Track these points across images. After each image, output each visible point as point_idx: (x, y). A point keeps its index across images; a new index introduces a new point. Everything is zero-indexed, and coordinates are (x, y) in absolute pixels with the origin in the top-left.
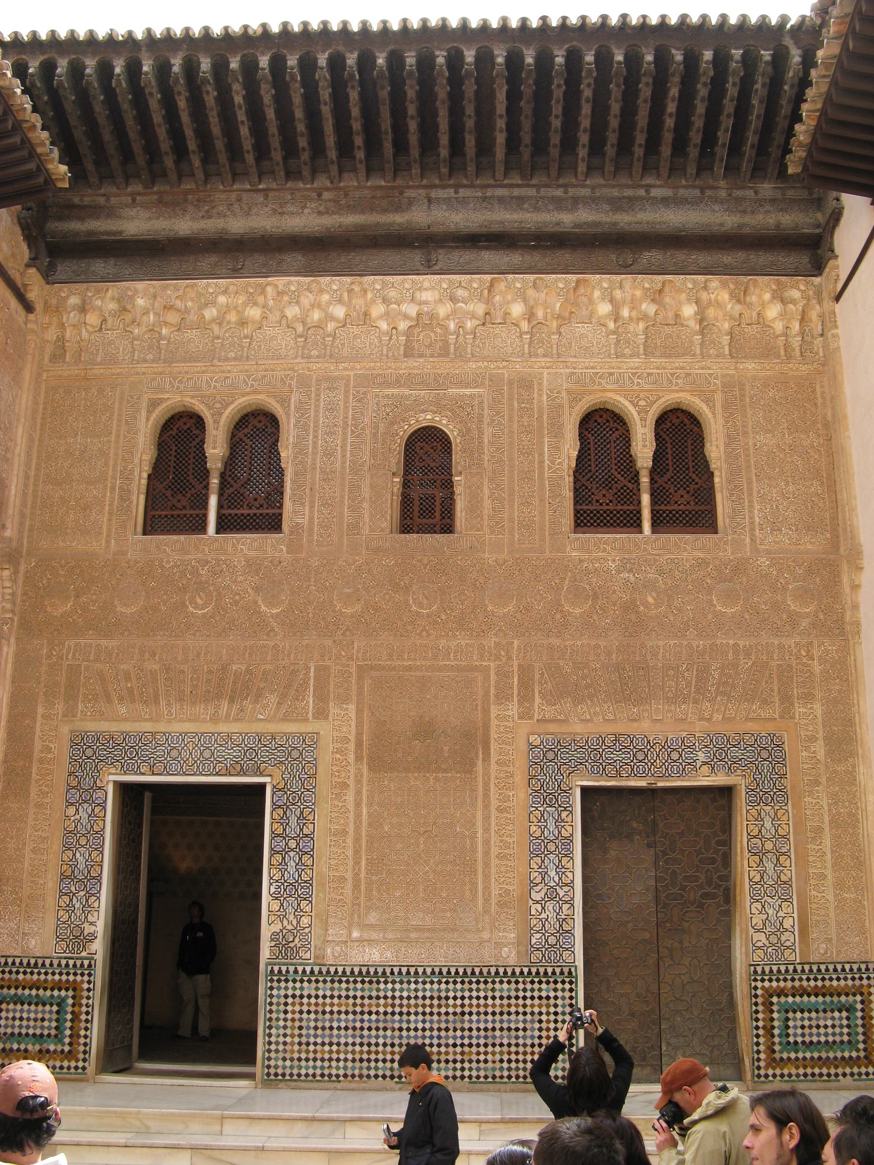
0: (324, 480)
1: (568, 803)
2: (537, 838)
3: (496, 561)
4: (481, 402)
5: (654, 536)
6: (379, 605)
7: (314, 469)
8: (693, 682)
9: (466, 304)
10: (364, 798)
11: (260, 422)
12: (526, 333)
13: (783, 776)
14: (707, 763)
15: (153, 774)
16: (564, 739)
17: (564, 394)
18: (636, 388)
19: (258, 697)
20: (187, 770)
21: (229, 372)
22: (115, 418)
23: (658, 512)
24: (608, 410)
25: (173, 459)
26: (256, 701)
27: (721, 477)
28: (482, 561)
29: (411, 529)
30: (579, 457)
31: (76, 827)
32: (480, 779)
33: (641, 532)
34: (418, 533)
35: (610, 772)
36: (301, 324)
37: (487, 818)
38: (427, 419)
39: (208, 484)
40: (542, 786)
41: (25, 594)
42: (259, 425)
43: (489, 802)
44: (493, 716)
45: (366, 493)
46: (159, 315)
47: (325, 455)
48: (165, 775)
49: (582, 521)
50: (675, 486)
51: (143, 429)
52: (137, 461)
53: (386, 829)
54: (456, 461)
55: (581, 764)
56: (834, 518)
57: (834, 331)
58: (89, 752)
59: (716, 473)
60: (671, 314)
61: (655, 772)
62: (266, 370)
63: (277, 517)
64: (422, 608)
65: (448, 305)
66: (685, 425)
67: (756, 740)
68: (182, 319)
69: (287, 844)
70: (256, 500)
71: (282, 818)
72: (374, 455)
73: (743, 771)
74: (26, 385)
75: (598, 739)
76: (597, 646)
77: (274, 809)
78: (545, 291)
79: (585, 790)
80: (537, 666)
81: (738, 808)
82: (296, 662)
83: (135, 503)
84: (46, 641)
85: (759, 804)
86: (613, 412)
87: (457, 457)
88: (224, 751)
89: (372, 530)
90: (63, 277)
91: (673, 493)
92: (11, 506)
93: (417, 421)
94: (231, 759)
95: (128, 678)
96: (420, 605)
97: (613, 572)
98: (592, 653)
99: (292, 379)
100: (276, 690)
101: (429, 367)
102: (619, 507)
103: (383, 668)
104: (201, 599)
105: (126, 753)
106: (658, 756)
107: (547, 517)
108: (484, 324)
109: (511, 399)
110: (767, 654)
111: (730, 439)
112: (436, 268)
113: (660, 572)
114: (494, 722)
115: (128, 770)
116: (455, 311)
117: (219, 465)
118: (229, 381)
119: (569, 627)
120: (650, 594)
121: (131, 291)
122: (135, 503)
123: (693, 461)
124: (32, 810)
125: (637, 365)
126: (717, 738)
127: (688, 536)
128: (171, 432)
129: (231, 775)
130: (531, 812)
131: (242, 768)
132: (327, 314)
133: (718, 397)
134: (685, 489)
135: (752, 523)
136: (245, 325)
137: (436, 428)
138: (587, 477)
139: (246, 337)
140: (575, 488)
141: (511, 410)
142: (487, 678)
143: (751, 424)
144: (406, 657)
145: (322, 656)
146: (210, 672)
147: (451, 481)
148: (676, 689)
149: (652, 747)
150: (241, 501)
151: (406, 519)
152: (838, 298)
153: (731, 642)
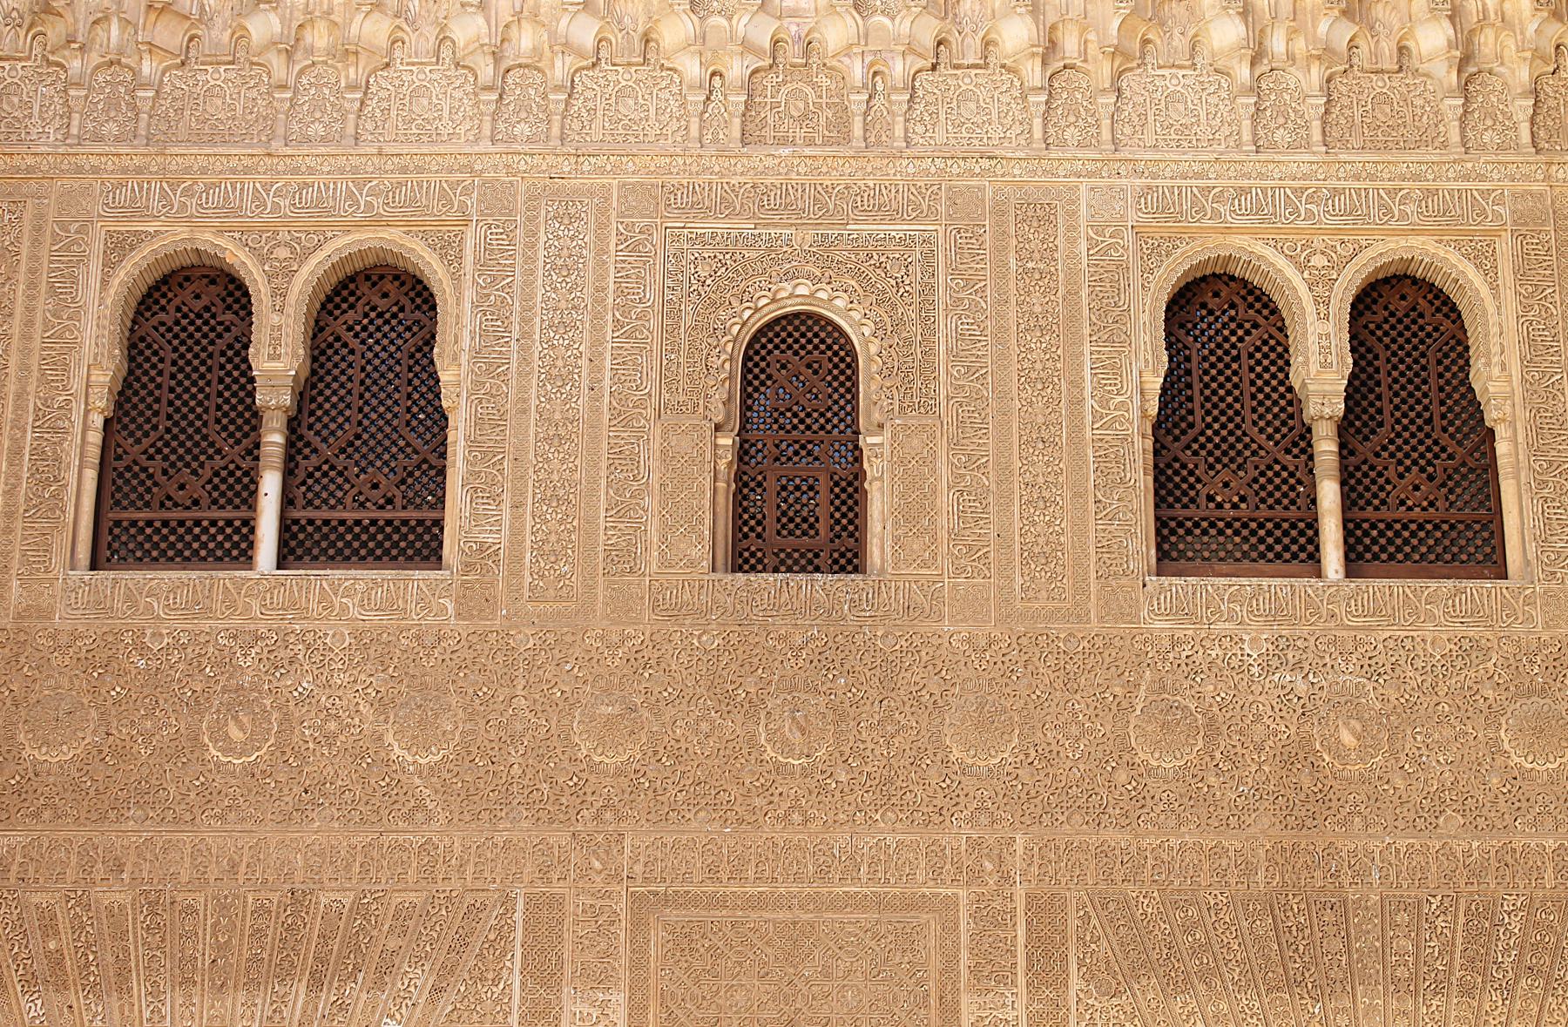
3: (969, 641)
5: (1353, 584)
7: (524, 411)
8: (1459, 941)
9: (893, 19)
11: (385, 295)
17: (1129, 236)
18: (1303, 224)
19: (385, 971)
21: (311, 171)
22: (22, 277)
23: (1358, 526)
24: (1232, 278)
26: (379, 984)
27: (1514, 440)
30: (1164, 390)
34: (776, 570)
36: (490, 60)
38: (796, 295)
39: (257, 446)
42: (382, 304)
45: (653, 470)
46: (136, 27)
50: (1400, 463)
51: (93, 308)
52: (77, 385)
54: (867, 396)
59: (1501, 432)
60: (1388, 47)
62: (404, 170)
63: (428, 530)
65: (849, 20)
66: (1421, 315)
68: (191, 39)
70: (375, 486)
72: (668, 380)
76: (1217, 852)
80: (1074, 896)
82: (479, 885)
83: (71, 489)
86: (1244, 283)
87: (869, 386)
89: (665, 563)
91: (1395, 480)
93: (774, 300)
95: (49, 927)
96: (787, 748)
97: (1255, 670)
98: (1206, 867)
99: (467, 192)
101: (802, 170)
102: (1264, 512)
103: (695, 901)
104: (242, 728)
107: (1092, 535)
111: (1536, 349)
113: (1373, 672)
116: (866, 36)
117: (287, 399)
120: (1346, 724)
122: (71, 489)
125: (1305, 168)
127: (1433, 584)
128: (162, 316)
132: (553, 35)
133: (1505, 247)
134: (1423, 470)
136: (352, 58)
137: (817, 318)
139: (352, 87)
140: (1156, 466)
145: (544, 872)
146: (261, 910)
147: (856, 447)
148: (1416, 964)
150: (340, 487)
151: (746, 536)
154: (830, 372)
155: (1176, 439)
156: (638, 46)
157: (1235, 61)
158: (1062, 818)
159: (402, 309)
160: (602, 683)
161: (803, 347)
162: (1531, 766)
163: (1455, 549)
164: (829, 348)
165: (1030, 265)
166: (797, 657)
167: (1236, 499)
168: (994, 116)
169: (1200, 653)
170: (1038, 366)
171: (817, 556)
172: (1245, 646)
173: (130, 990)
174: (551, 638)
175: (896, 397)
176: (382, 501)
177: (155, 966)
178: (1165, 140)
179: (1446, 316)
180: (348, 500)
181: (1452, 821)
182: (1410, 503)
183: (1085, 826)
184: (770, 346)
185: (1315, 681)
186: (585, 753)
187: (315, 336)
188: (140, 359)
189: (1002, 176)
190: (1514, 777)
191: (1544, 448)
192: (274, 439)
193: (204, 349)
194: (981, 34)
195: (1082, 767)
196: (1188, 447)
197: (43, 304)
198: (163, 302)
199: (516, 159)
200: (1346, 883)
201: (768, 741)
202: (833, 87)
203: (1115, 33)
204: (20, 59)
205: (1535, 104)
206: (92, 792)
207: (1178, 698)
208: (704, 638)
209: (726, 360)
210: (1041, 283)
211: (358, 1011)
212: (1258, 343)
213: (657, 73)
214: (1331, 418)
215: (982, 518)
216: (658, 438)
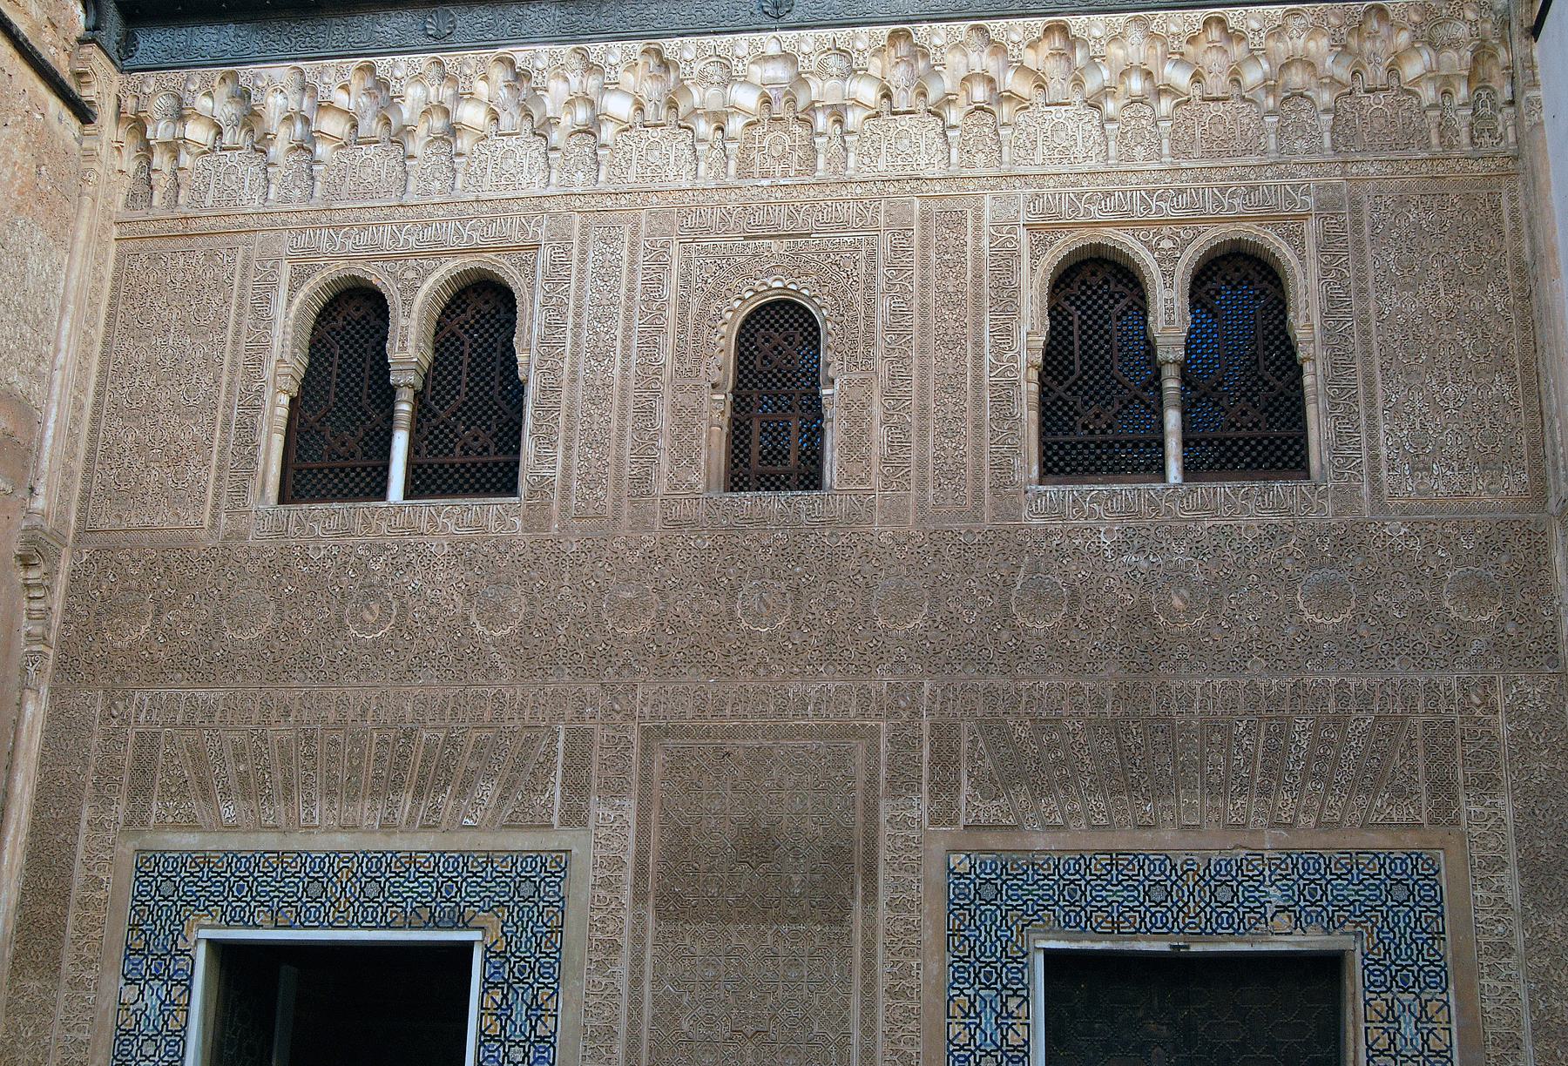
0: (592, 401)
1: (1021, 981)
2: (962, 1048)
4: (871, 255)
7: (574, 380)
8: (1260, 754)
10: (648, 970)
11: (487, 302)
13: (1439, 935)
14: (1285, 909)
15: (277, 927)
16: (1015, 861)
17: (1023, 234)
20: (336, 920)
22: (234, 301)
25: (335, 370)
26: (461, 794)
28: (868, 538)
29: (746, 484)
31: (138, 1023)
32: (858, 936)
33: (1164, 480)
34: (758, 490)
35: (1099, 924)
37: (869, 1007)
38: (776, 285)
40: (972, 949)
41: (68, 610)
43: (874, 978)
44: (883, 817)
45: (664, 419)
47: (594, 356)
48: (297, 928)
49: (1056, 465)
53: (685, 1027)
55: (1046, 908)
56: (1537, 445)
57: (1530, 94)
58: (167, 888)
59: (1307, 367)
61: (1186, 926)
64: (759, 624)
67: (1382, 866)
69: (506, 1054)
70: (476, 439)
71: (499, 1007)
73: (1358, 924)
74: (79, 246)
75: (1077, 862)
76: (1077, 690)
77: (486, 991)
79: (1054, 959)
81: (1349, 997)
82: (533, 723)
84: (101, 692)
85: (1389, 989)
86: (1114, 264)
88: (402, 885)
90: (145, 62)
92: (46, 456)
94: (414, 899)
96: (757, 618)
100: (496, 774)
101: (779, 195)
103: (688, 733)
104: (372, 613)
105: (230, 889)
106: (1191, 894)
107: (987, 456)
108: (877, 115)
109: (924, 247)
110: (1405, 700)
111: (1333, 305)
112: (789, 17)
113: (1197, 550)
114: (885, 830)
115: (232, 919)
117: (411, 378)
118: (429, 232)
119: (1025, 655)
120: (1177, 593)
121: (262, 80)
124: (63, 993)
126: (1305, 861)
129: (411, 928)
130: (951, 998)
131: (432, 915)
133: (1311, 227)
138: (1066, 384)
141: (924, 267)
142: (873, 751)
143: (1372, 273)
144: (728, 712)
148: (1227, 770)
149: (1180, 878)
150: (451, 441)
152: (1535, 31)
153: (1333, 680)
154: (801, 343)
155: (1061, 383)
158: (958, 668)
159: (498, 312)
160: (625, 575)
161: (781, 326)
163: (1286, 459)
164: (801, 325)
165: (947, 257)
167: (1104, 426)
168: (923, 148)
171: (788, 478)
173: (292, 799)
176: (480, 450)
177: (308, 782)
179: (1271, 283)
180: (457, 450)
181: (1256, 665)
182: (1238, 425)
184: (757, 326)
187: (436, 333)
188: (318, 355)
190: (1304, 628)
192: (404, 408)
193: (361, 346)
197: (248, 320)
198: (335, 314)
199: (573, 198)
200: (1174, 712)
201: (744, 615)
204: (237, 149)
206: (270, 661)
209: (726, 336)
211: (448, 813)
213: (677, 131)
214: (1175, 362)
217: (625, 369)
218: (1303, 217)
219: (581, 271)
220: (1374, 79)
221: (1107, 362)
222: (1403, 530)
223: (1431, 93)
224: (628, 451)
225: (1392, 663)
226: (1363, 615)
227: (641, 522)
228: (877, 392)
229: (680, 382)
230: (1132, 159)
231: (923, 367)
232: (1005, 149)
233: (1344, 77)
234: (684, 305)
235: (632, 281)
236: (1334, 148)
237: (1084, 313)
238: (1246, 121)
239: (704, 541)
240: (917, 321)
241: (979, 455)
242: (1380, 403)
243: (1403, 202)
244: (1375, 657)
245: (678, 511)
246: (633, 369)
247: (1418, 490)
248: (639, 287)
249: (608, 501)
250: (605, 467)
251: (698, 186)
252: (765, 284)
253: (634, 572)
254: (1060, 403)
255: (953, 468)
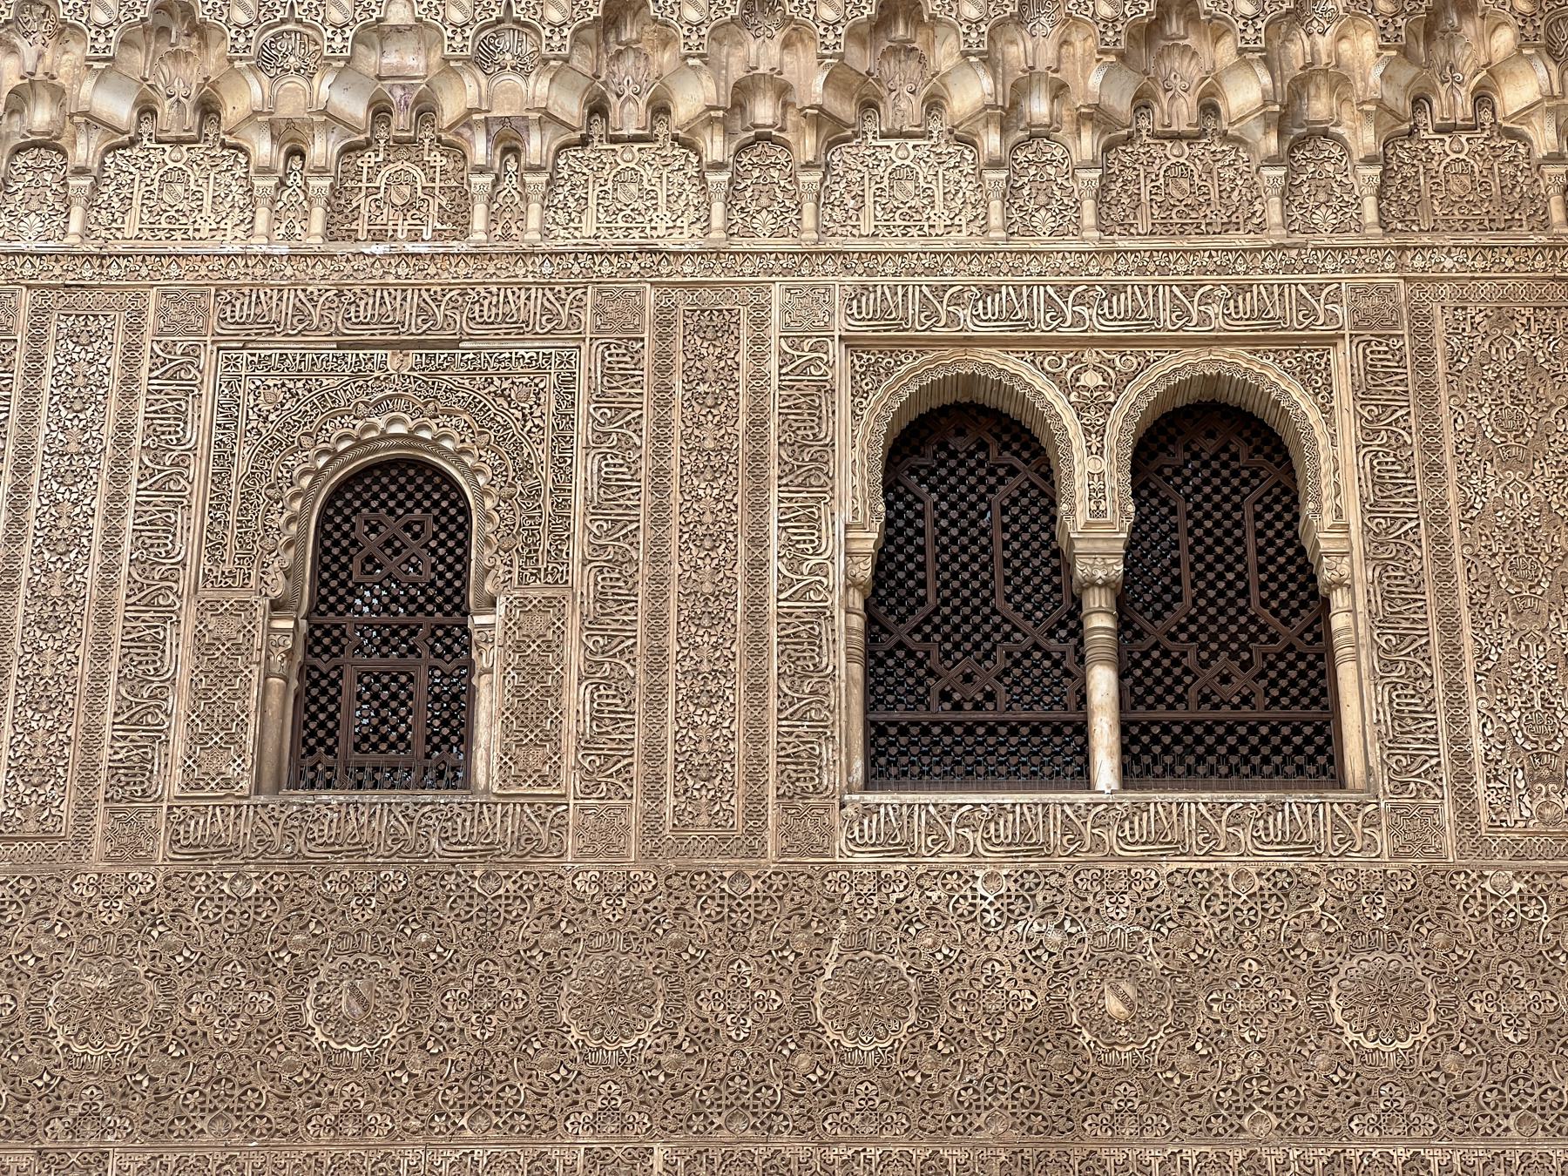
6: (201, 1027)
12: (718, 166)
17: (836, 350)
18: (1066, 332)
23: (1145, 730)
28: (554, 883)
47: (50, 544)
59: (1339, 599)
64: (347, 1037)
66: (1235, 457)
78: (779, 36)
96: (342, 1027)
107: (772, 739)
108: (584, 142)
109: (663, 369)
113: (1151, 916)
116: (490, 99)
119: (840, 1098)
123: (1262, 569)
125: (1072, 260)
127: (1239, 798)
133: (1342, 359)
135: (1462, 757)
138: (912, 621)
141: (664, 404)
151: (311, 751)
153: (1401, 1153)
154: (435, 535)
156: (192, 119)
157: (980, 125)
158: (718, 1121)
160: (92, 946)
162: (1371, 1045)
165: (702, 388)
166: (363, 906)
167: (979, 697)
168: (662, 200)
169: (916, 896)
170: (708, 518)
172: (978, 885)
174: (26, 886)
175: (516, 564)
178: (888, 227)
179: (1269, 457)
182: (1216, 699)
183: (749, 1132)
184: (357, 504)
185: (1073, 930)
186: (62, 1041)
189: (668, 275)
191: (1393, 618)
194: (646, 97)
195: (748, 1050)
196: (918, 629)
201: (318, 1021)
202: (450, 168)
203: (819, 89)
205: (1382, 174)
207: (883, 956)
208: (239, 883)
210: (715, 412)
212: (1016, 494)
214: (1106, 584)
215: (624, 720)
216: (192, 621)
217: (109, 569)
218: (1332, 340)
219: (31, 392)
220: (1452, 108)
221: (985, 584)
222: (1517, 886)
223: (1551, 135)
224: (109, 717)
225: (1505, 1123)
226: (1450, 1037)
227: (129, 849)
228: (574, 623)
229: (214, 596)
230: (1031, 231)
231: (659, 580)
232: (809, 208)
233: (1401, 103)
234: (224, 457)
235: (126, 413)
236: (1383, 224)
237: (943, 497)
238: (1230, 173)
239: (249, 883)
240: (647, 499)
241: (756, 736)
242: (1469, 664)
243: (1503, 318)
244: (1474, 1113)
245: (197, 829)
246: (125, 569)
247: (1541, 816)
248: (141, 423)
249: (67, 809)
250: (63, 745)
251: (256, 249)
252: (373, 427)
253: (112, 940)
254: (901, 654)
255: (711, 759)
